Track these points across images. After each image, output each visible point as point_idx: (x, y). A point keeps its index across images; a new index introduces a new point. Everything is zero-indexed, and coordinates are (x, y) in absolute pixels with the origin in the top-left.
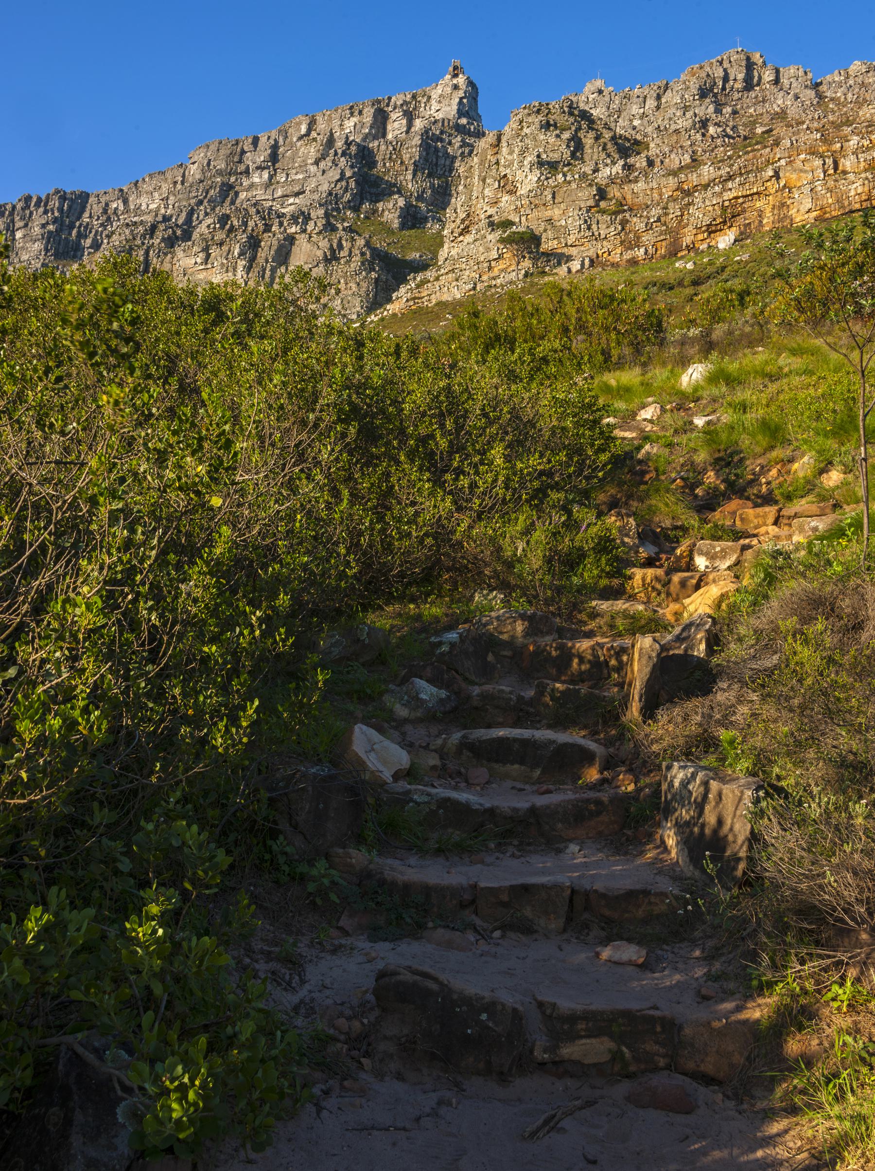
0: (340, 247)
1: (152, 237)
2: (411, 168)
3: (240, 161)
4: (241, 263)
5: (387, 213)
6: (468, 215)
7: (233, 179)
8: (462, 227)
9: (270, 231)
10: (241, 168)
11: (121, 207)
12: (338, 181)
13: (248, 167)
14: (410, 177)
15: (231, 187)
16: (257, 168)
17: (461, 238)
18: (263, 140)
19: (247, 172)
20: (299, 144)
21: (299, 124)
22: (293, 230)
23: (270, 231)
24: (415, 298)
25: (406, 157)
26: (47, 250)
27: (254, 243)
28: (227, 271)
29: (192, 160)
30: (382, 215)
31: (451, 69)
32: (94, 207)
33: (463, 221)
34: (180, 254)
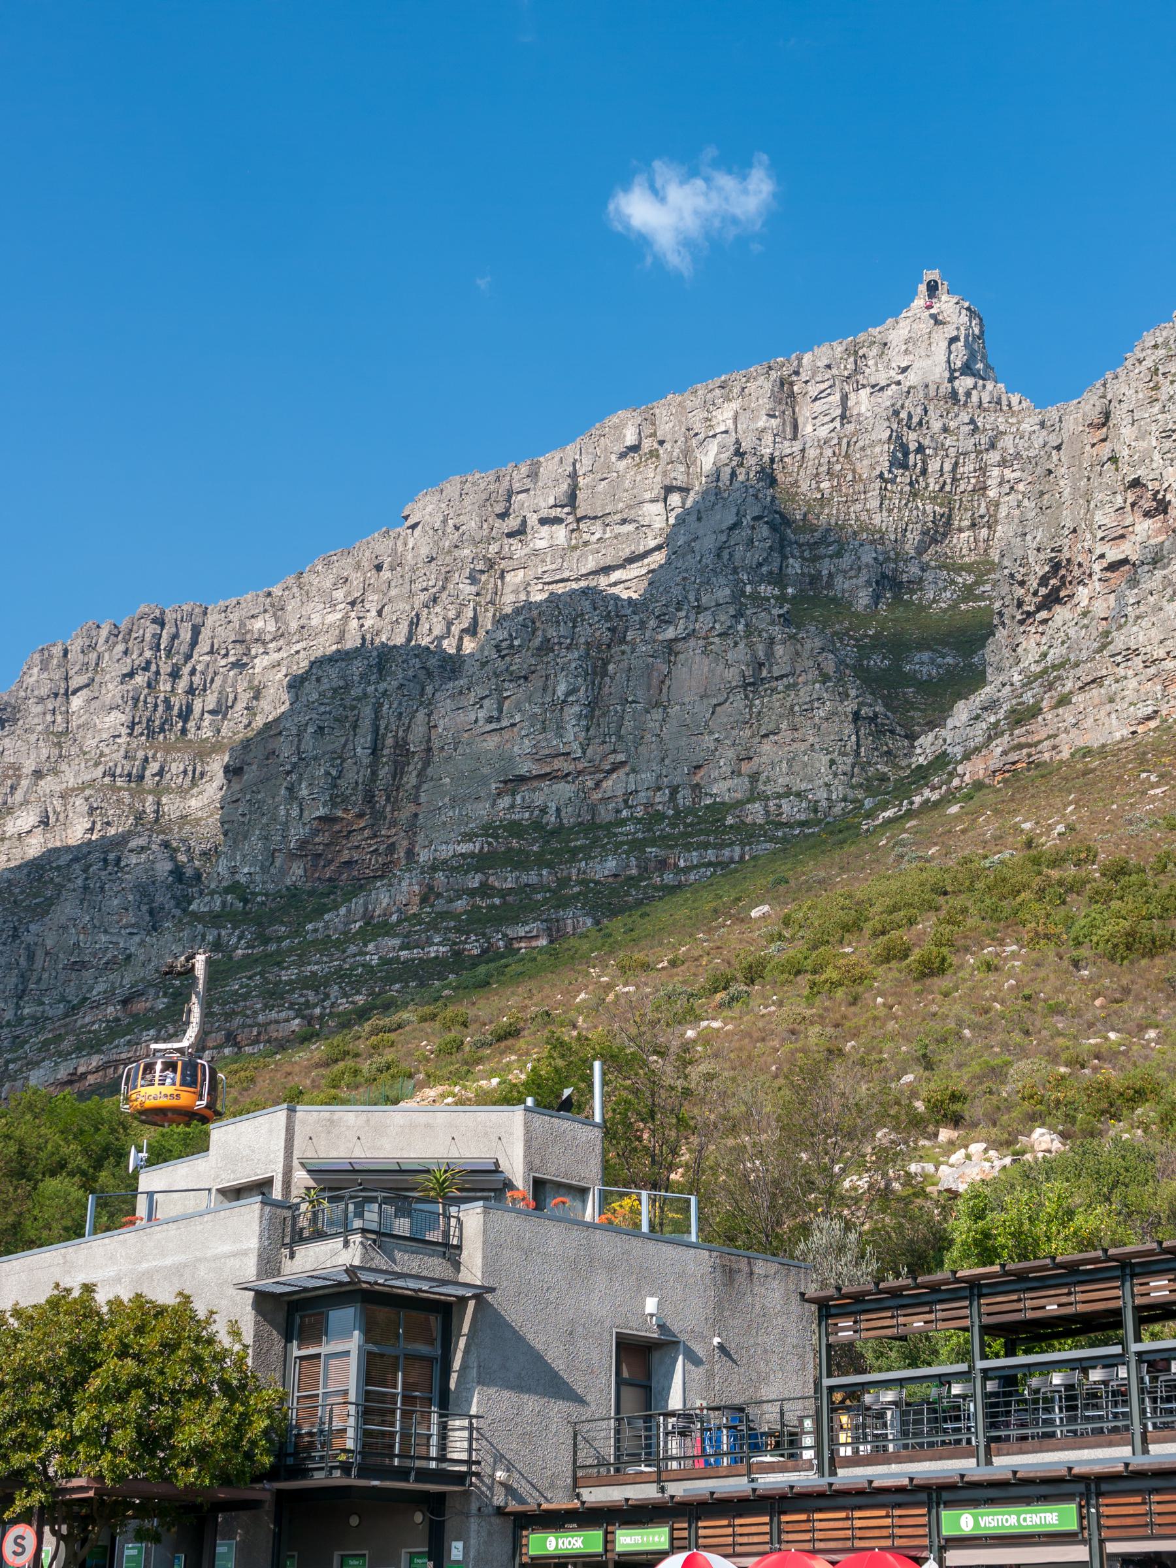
1: (381, 678)
5: (839, 580)
6: (1056, 566)
8: (1043, 591)
9: (623, 640)
12: (732, 528)
13: (524, 522)
16: (543, 521)
17: (1043, 614)
20: (622, 465)
23: (623, 640)
24: (1020, 747)
25: (863, 468)
28: (544, 729)
29: (410, 522)
30: (830, 586)
31: (922, 288)
33: (1044, 581)
34: (445, 704)
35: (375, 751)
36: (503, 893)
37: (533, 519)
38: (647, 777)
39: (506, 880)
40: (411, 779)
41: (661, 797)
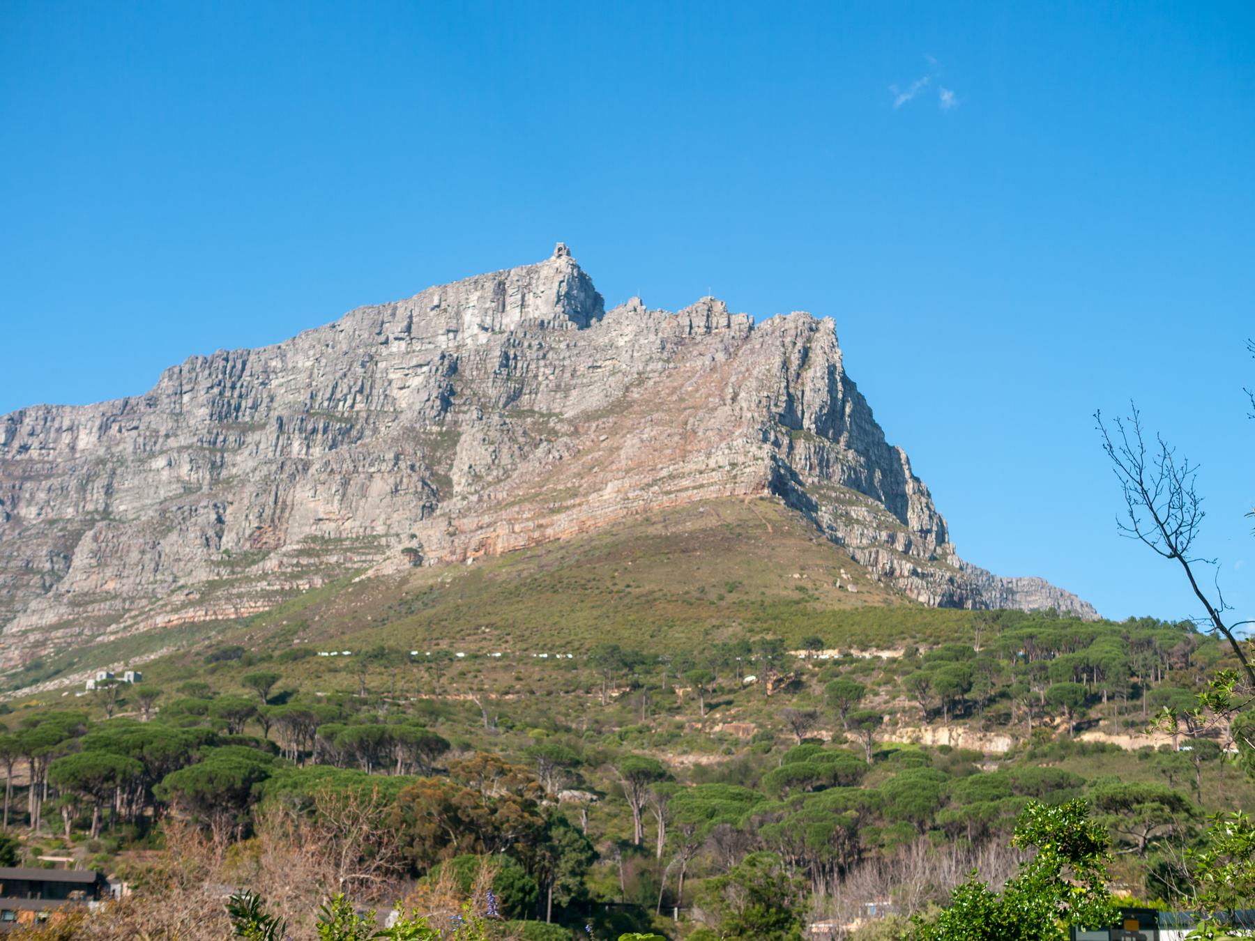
0: (401, 481)
2: (492, 376)
3: (379, 334)
4: (337, 497)
7: (374, 350)
10: (382, 338)
11: (280, 365)
14: (490, 384)
15: (371, 358)
18: (400, 312)
19: (386, 342)
20: (432, 313)
21: (432, 295)
22: (372, 470)
25: (489, 366)
26: (211, 416)
27: (345, 483)
32: (254, 364)
35: (276, 502)
36: (302, 566)
37: (391, 337)
38: (358, 523)
39: (304, 561)
40: (287, 515)
41: (361, 530)
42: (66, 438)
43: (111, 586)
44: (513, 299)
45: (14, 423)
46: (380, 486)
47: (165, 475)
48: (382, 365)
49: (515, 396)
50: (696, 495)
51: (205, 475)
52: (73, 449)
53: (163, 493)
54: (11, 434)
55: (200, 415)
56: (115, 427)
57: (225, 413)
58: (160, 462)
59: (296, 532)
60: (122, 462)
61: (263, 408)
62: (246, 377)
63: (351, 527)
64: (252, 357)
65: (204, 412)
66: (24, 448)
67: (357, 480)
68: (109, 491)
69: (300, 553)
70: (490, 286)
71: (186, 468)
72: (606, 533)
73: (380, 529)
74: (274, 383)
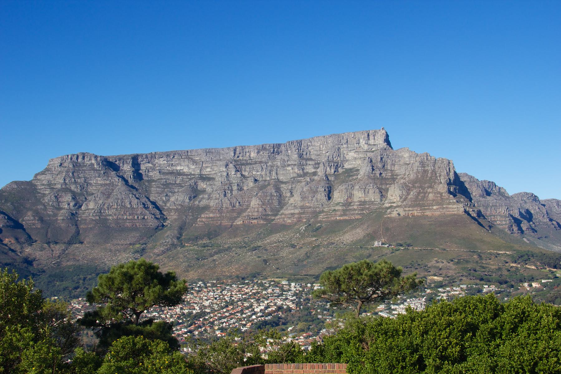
42: (248, 154)
43: (307, 204)
44: (371, 137)
45: (235, 150)
46: (370, 191)
47: (291, 171)
48: (342, 150)
49: (384, 166)
50: (453, 213)
51: (301, 172)
52: (250, 157)
53: (292, 176)
54: (235, 153)
55: (295, 156)
56: (262, 152)
57: (301, 156)
58: (290, 168)
59: (356, 199)
60: (278, 167)
61: (308, 154)
62: (302, 146)
63: (367, 199)
64: (303, 142)
65: (296, 156)
66: (238, 157)
67: (367, 190)
68: (277, 173)
69: (360, 205)
70: (366, 135)
71: (296, 170)
72: (391, 184)
73: (373, 200)
74: (310, 148)
